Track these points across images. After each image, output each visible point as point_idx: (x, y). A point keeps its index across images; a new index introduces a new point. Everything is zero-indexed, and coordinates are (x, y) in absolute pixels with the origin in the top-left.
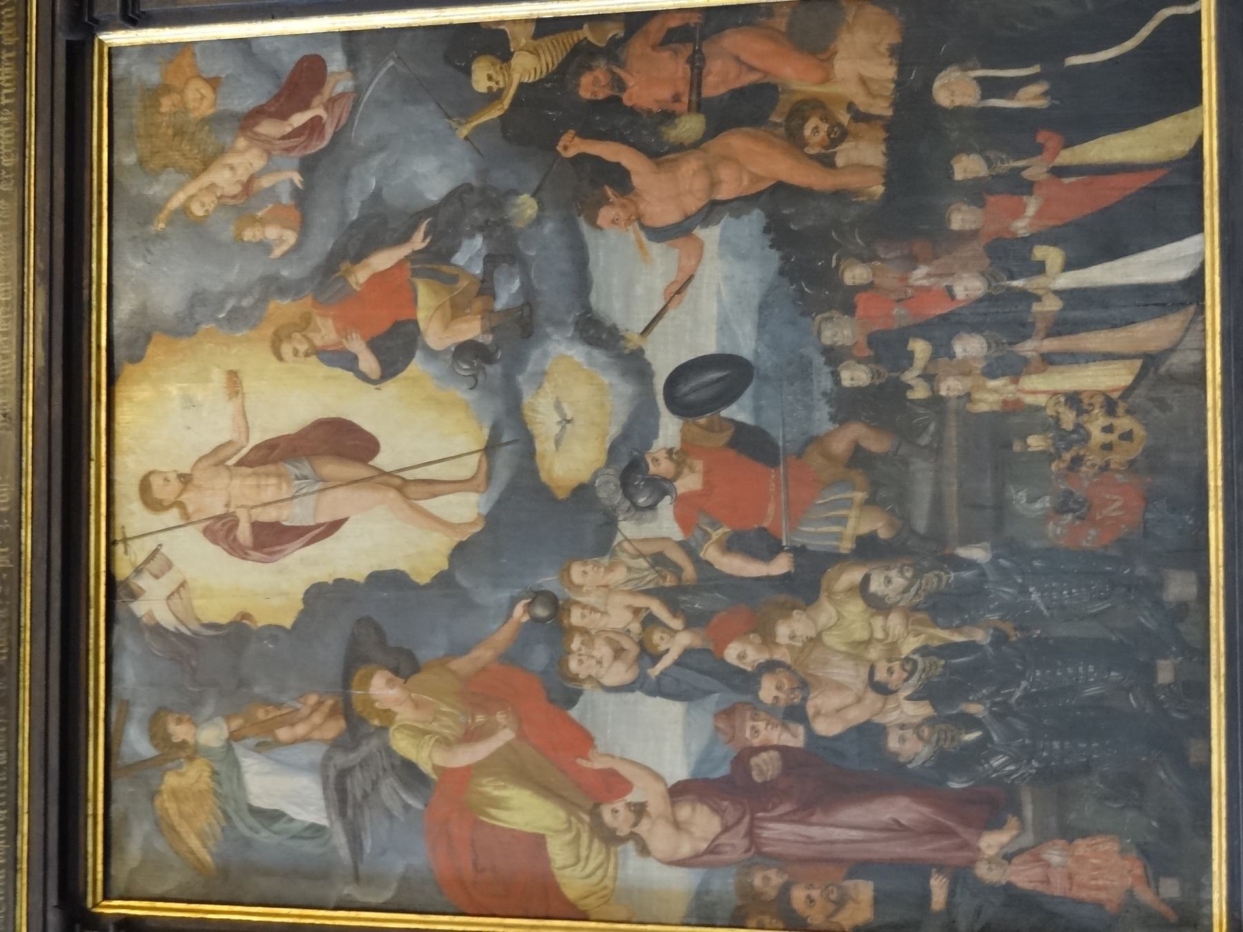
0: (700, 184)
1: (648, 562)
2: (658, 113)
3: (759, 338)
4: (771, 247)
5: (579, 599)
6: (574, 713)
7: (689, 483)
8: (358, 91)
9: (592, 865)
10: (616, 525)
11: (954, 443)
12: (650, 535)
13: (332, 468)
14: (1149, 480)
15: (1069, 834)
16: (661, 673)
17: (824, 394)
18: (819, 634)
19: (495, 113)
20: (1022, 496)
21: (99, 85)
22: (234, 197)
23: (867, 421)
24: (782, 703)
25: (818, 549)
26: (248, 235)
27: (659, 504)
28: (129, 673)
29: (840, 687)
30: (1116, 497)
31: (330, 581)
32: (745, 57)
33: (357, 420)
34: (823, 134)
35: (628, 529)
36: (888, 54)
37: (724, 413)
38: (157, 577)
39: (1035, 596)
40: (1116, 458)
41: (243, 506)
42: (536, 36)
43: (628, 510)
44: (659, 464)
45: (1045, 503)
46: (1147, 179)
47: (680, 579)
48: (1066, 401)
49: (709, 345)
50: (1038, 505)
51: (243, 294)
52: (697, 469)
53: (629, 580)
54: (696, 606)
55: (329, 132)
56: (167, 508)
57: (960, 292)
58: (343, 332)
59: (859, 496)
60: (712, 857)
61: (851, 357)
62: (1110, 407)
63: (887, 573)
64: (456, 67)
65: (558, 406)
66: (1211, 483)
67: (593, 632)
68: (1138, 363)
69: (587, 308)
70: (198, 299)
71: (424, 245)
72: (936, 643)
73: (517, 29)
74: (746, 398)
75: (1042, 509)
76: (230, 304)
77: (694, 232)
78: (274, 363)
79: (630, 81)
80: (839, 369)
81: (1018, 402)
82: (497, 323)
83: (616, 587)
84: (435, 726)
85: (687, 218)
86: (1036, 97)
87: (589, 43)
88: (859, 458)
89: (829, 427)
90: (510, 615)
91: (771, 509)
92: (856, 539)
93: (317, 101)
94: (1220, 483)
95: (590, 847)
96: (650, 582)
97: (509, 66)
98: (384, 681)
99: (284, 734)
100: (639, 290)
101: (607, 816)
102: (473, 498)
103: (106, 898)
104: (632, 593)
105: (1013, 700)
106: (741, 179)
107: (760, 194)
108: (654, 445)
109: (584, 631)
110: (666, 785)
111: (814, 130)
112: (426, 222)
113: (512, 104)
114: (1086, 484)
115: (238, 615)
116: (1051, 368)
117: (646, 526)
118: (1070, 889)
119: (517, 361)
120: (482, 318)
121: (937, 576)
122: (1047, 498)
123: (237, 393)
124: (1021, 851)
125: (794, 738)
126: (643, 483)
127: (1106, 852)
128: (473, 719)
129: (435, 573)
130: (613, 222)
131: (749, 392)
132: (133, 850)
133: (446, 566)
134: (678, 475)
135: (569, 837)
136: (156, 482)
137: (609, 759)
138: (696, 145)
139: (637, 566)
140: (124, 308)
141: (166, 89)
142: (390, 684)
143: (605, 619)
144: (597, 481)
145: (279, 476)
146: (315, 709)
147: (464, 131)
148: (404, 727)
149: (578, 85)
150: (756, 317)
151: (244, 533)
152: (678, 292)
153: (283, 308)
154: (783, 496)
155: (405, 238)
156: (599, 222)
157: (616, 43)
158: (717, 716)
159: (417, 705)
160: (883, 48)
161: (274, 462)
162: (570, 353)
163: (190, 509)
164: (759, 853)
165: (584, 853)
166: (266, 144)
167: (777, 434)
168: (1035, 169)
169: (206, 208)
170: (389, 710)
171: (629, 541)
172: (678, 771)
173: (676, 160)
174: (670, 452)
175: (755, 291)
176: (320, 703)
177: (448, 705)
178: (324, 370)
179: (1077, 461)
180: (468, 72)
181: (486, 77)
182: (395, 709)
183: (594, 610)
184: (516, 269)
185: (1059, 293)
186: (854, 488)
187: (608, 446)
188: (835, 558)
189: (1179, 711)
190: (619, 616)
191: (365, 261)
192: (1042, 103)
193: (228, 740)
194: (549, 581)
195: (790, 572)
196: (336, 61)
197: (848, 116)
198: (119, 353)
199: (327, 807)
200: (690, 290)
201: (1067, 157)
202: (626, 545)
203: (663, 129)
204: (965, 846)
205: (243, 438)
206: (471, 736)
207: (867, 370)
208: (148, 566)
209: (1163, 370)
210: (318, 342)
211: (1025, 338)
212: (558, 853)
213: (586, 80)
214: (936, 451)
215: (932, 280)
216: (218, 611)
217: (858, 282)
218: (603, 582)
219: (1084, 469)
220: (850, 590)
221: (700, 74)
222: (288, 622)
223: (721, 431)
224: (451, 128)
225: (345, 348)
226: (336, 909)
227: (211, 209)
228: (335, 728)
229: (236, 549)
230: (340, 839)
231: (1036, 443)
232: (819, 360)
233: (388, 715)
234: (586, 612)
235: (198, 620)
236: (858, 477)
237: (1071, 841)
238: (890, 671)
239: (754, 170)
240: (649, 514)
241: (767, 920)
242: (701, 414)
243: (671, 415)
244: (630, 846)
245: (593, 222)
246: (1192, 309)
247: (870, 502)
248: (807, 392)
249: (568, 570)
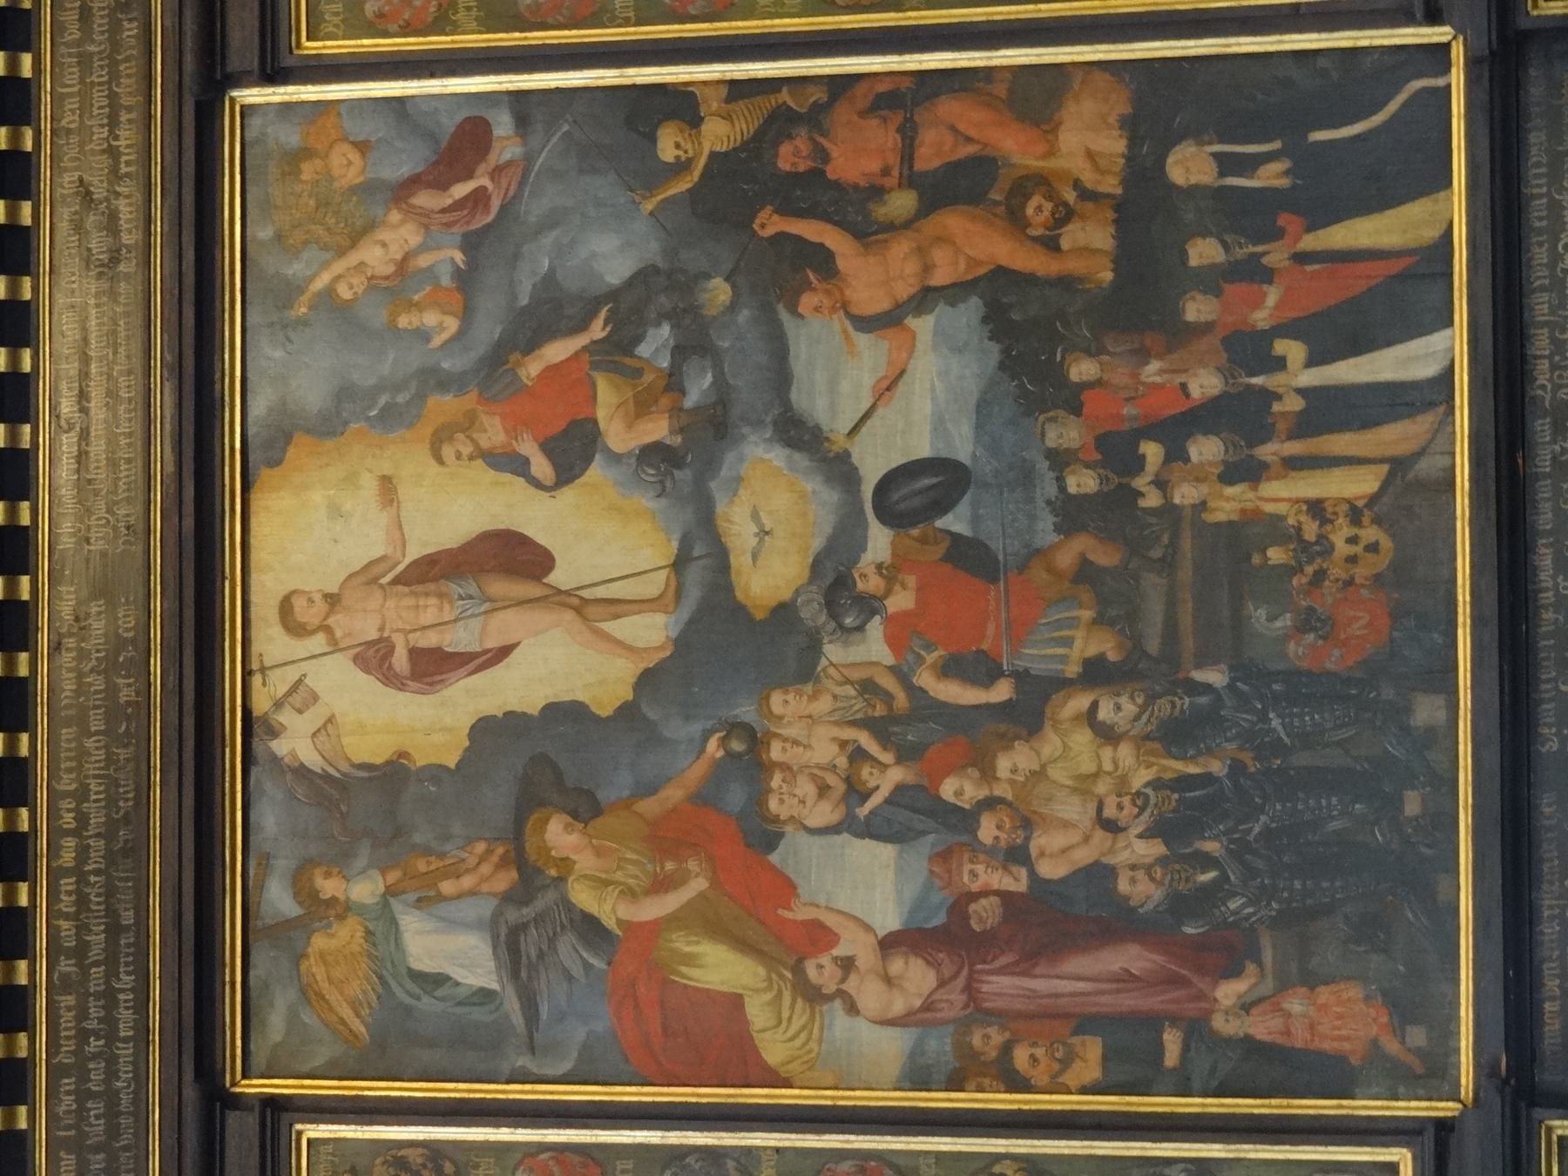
0: (912, 267)
2: (865, 188)
3: (978, 440)
4: (990, 339)
5: (779, 731)
6: (774, 858)
7: (901, 601)
8: (529, 159)
9: (795, 1026)
11: (1189, 555)
12: (858, 659)
13: (500, 587)
14: (1396, 595)
15: (1311, 980)
16: (871, 812)
17: (1049, 502)
18: (1043, 767)
19: (682, 185)
20: (1261, 613)
21: (231, 150)
22: (387, 278)
24: (1003, 844)
26: (403, 321)
28: (269, 819)
29: (1066, 825)
30: (1361, 614)
31: (500, 715)
32: (961, 127)
33: (530, 532)
34: (1046, 213)
35: (833, 652)
36: (1116, 125)
37: (940, 523)
38: (300, 712)
39: (1276, 723)
40: (1361, 572)
41: (398, 630)
42: (728, 100)
45: (1285, 621)
46: (1396, 266)
47: (890, 707)
48: (1308, 511)
49: (923, 449)
50: (1278, 624)
51: (397, 388)
53: (834, 710)
54: (909, 737)
55: (496, 204)
56: (313, 632)
57: (1196, 392)
58: (513, 432)
59: (1087, 614)
60: (928, 1015)
61: (1078, 460)
62: (1355, 516)
63: (1117, 699)
64: (640, 133)
65: (755, 516)
66: (1460, 598)
67: (795, 768)
68: (1385, 468)
69: (787, 405)
70: (345, 393)
71: (604, 334)
72: (1168, 776)
73: (707, 90)
74: (963, 508)
75: (1283, 628)
76: (383, 400)
77: (906, 321)
78: (434, 468)
79: (835, 152)
81: (1257, 512)
82: (687, 423)
84: (619, 876)
85: (898, 306)
86: (1278, 176)
87: (789, 108)
88: (1085, 573)
89: (1054, 538)
90: (702, 750)
91: (991, 630)
93: (482, 169)
94: (1468, 598)
95: (792, 1007)
97: (699, 133)
98: (561, 826)
99: (447, 887)
100: (845, 386)
101: (811, 972)
102: (660, 619)
103: (244, 1076)
104: (836, 723)
105: (1251, 838)
106: (957, 263)
107: (976, 281)
109: (785, 767)
110: (876, 936)
111: (1037, 209)
112: (606, 309)
113: (703, 176)
114: (1330, 600)
115: (394, 753)
116: (1293, 474)
117: (852, 649)
118: (1312, 1041)
119: (710, 465)
120: (670, 417)
122: (1288, 615)
123: (392, 501)
124: (1260, 1001)
125: (1015, 882)
127: (1349, 1000)
128: (662, 868)
129: (618, 704)
130: (817, 309)
132: (275, 1025)
133: (631, 698)
134: (888, 592)
135: (769, 996)
136: (299, 603)
137: (816, 909)
138: (908, 224)
140: (258, 408)
141: (306, 153)
142: (568, 828)
143: (809, 753)
145: (441, 596)
146: (482, 859)
147: (649, 206)
148: (585, 877)
149: (776, 155)
150: (974, 417)
151: (400, 660)
152: (888, 389)
153: (444, 406)
154: (1003, 615)
155: (582, 326)
156: (800, 310)
157: (818, 109)
158: (931, 859)
159: (599, 852)
160: (1112, 119)
161: (435, 579)
162: (767, 456)
163: (339, 633)
164: (979, 1009)
165: (785, 1014)
166: (424, 218)
167: (996, 545)
168: (1276, 255)
169: (356, 289)
170: (567, 858)
171: (834, 666)
172: (889, 920)
173: (886, 241)
174: (879, 567)
175: (972, 389)
176: (489, 852)
177: (634, 851)
178: (492, 474)
179: (1320, 575)
180: (652, 139)
181: (672, 145)
182: (573, 857)
183: (796, 743)
184: (708, 363)
185: (1301, 391)
186: (1081, 607)
187: (811, 560)
188: (1061, 684)
189: (1428, 846)
190: (823, 749)
191: (537, 352)
192: (1284, 182)
193: (384, 895)
194: (746, 711)
195: (1011, 699)
196: (503, 124)
197: (1075, 194)
198: (253, 457)
199: (498, 968)
200: (901, 387)
201: (1310, 242)
202: (832, 671)
203: (871, 206)
204: (1201, 996)
205: (399, 554)
206: (661, 885)
207: (1095, 476)
208: (290, 699)
209: (1411, 476)
210: (485, 443)
211: (1263, 442)
212: (757, 1013)
213: (785, 149)
214: (1167, 564)
215: (1166, 377)
216: (369, 748)
217: (1084, 378)
218: (806, 713)
219: (1327, 583)
220: (1077, 718)
221: (911, 146)
222: (452, 763)
224: (634, 202)
225: (514, 450)
226: (508, 1082)
227: (360, 292)
228: (506, 880)
229: (391, 679)
230: (512, 1005)
231: (1276, 555)
232: (1043, 465)
233: (566, 864)
234: (788, 745)
235: (348, 759)
236: (1086, 595)
237: (1312, 989)
238: (1120, 807)
239: (971, 253)
240: (856, 636)
241: (986, 1082)
242: (914, 525)
244: (838, 1004)
245: (793, 310)
246: (1442, 409)
247: (1099, 621)
248: (1030, 500)
249: (768, 698)
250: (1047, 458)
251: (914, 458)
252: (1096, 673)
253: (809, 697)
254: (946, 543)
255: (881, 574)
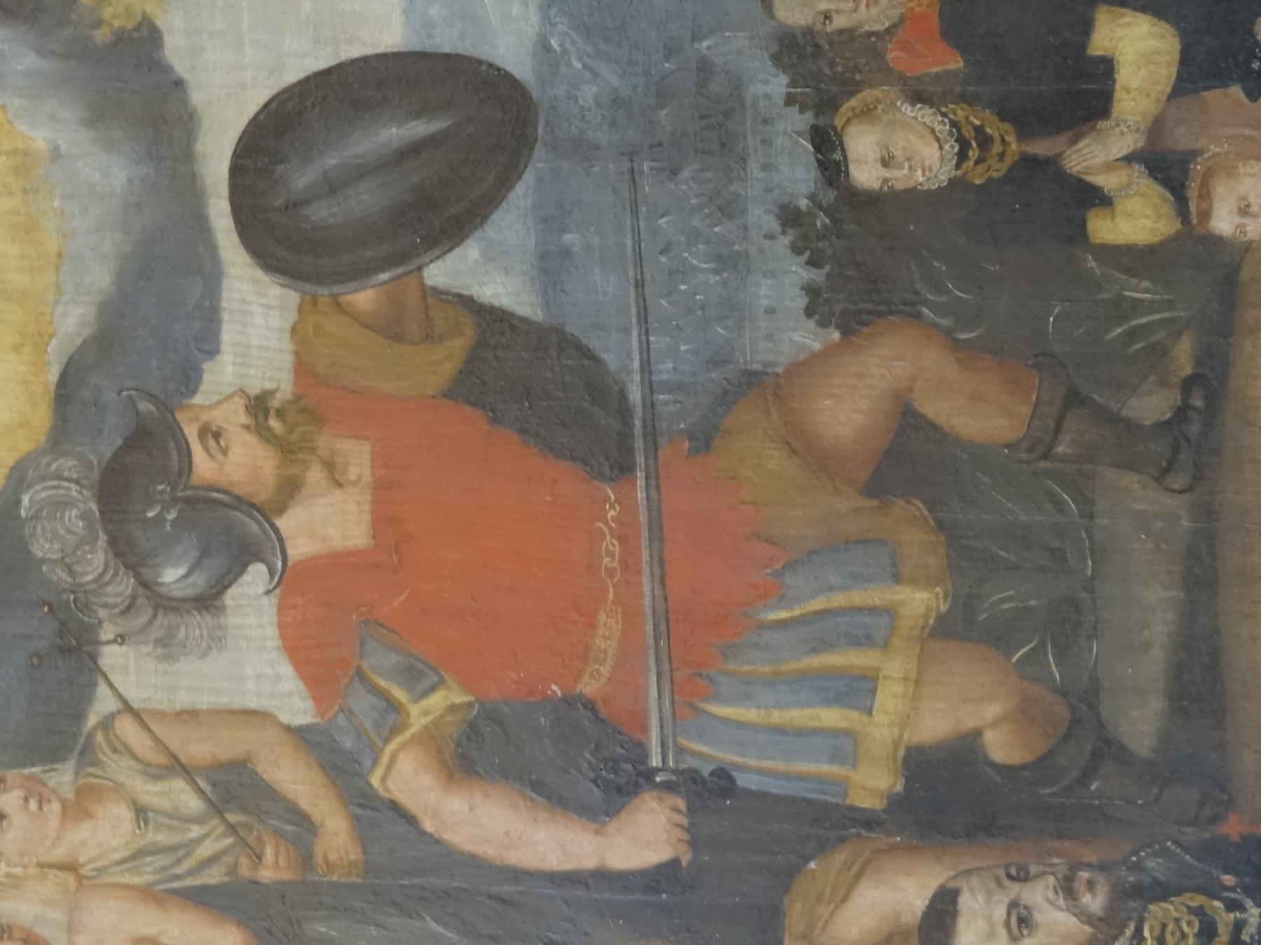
1: (202, 793)
10: (94, 658)
12: (203, 701)
17: (790, 217)
23: (944, 322)
25: (776, 787)
27: (233, 591)
43: (129, 609)
44: (225, 452)
47: (306, 860)
52: (352, 476)
61: (885, 73)
80: (839, 122)
83: (101, 871)
91: (608, 626)
92: (907, 760)
96: (211, 861)
104: (147, 893)
108: (206, 377)
117: (187, 666)
121: (1199, 912)
126: (172, 515)
131: (522, 194)
134: (289, 490)
139: (166, 805)
144: (26, 500)
171: (136, 714)
174: (259, 406)
187: (53, 375)
195: (674, 863)
202: (127, 728)
207: (943, 129)
218: (59, 853)
223: (429, 337)
240: (196, 625)
242: (358, 273)
243: (259, 273)
248: (730, 209)
250: (776, 59)
251: (356, 52)
253: (64, 804)
254: (459, 345)
255: (260, 428)
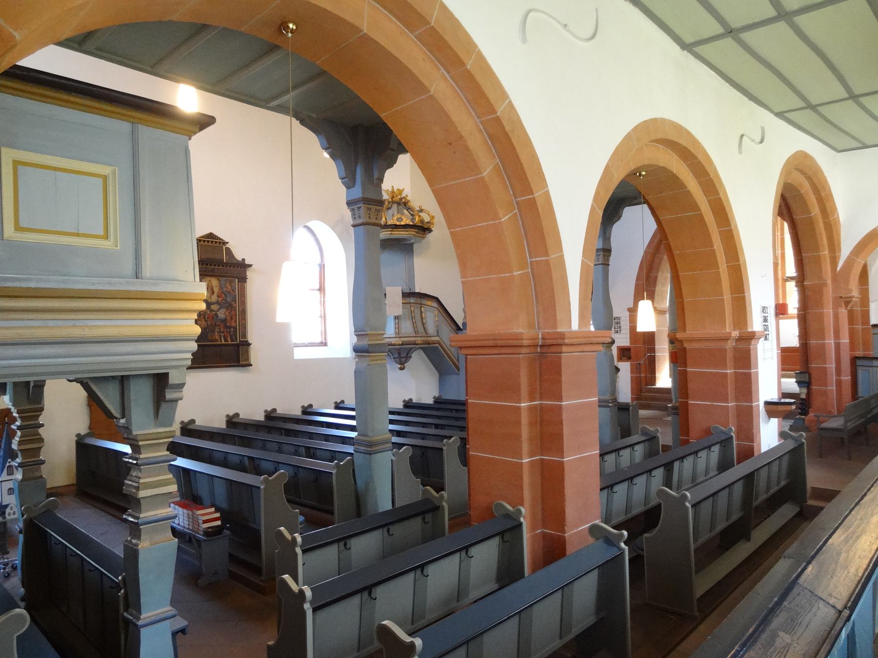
252: (208, 324)
